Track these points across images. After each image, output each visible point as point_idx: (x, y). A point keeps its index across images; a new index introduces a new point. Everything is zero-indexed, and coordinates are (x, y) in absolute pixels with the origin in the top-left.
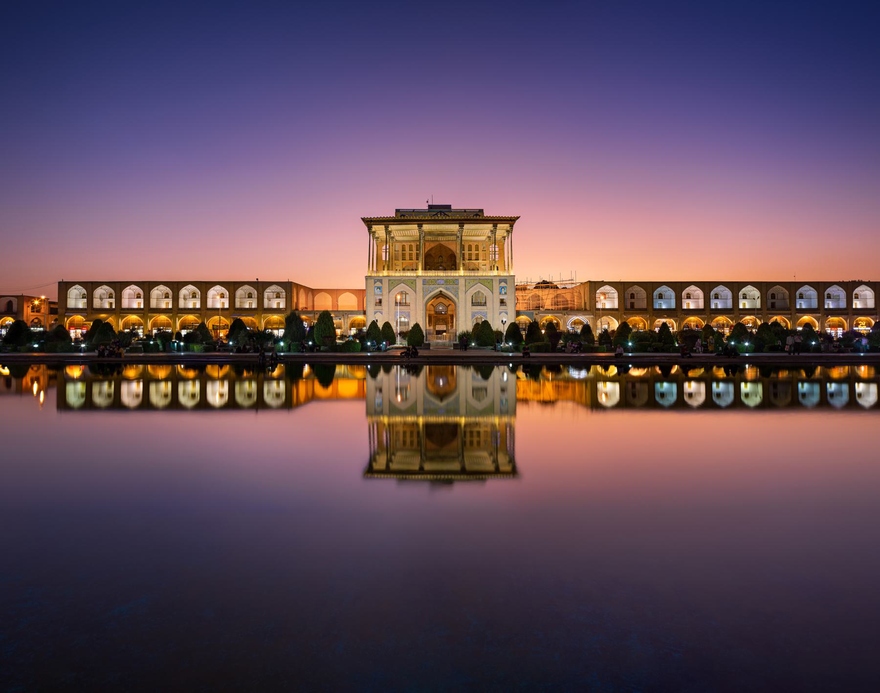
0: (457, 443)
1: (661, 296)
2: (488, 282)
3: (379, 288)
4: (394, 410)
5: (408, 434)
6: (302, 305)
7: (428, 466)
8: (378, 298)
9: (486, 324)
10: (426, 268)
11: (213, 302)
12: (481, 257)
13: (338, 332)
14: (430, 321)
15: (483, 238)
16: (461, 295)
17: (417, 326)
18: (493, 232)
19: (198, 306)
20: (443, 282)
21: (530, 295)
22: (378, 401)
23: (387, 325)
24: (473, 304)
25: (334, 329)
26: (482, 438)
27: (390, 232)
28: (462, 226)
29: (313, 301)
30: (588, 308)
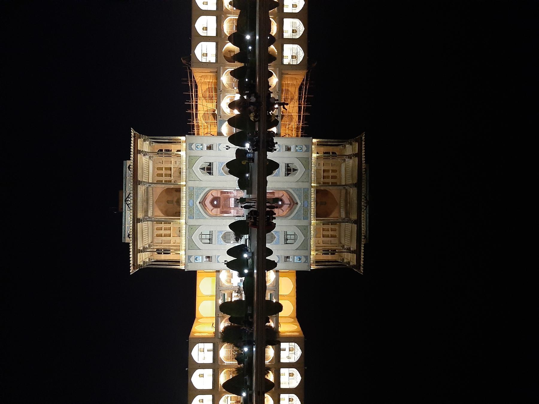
0: (333, 190)
2: (191, 161)
3: (196, 259)
4: (305, 246)
5: (326, 233)
7: (354, 217)
8: (205, 259)
9: (229, 165)
12: (168, 166)
15: (151, 163)
16: (203, 184)
17: (231, 226)
18: (145, 154)
20: (191, 201)
21: (204, 122)
22: (296, 260)
23: (230, 252)
26: (330, 168)
28: (140, 183)
29: (207, 317)
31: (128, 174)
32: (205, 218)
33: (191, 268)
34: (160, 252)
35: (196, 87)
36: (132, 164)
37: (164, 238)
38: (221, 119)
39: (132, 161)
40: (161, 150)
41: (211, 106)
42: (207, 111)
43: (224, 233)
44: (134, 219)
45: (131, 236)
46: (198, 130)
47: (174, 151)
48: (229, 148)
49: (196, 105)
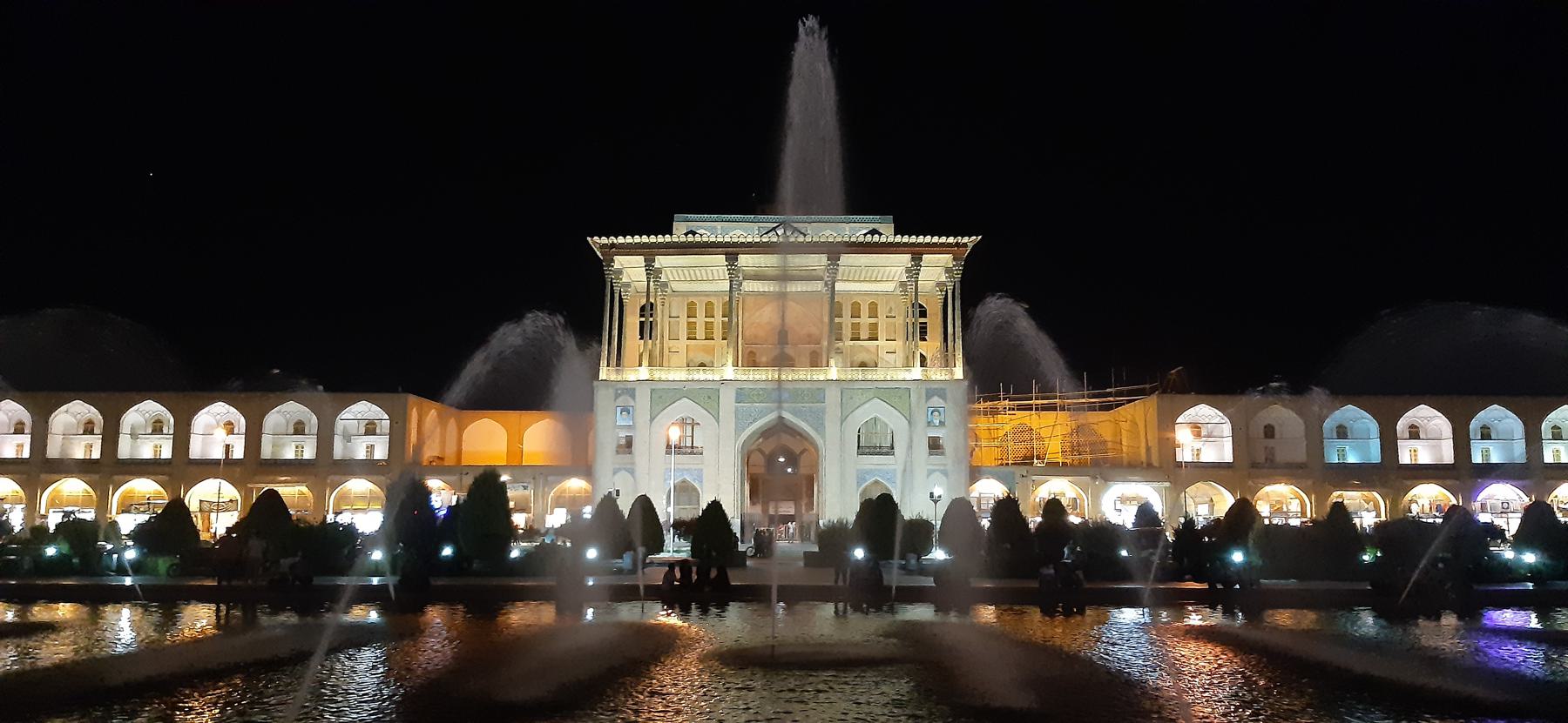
1: (1342, 433)
3: (625, 410)
6: (430, 452)
8: (623, 434)
10: (752, 361)
11: (205, 444)
12: (882, 334)
13: (519, 520)
14: (753, 493)
15: (889, 287)
16: (831, 428)
17: (715, 507)
18: (914, 272)
19: (167, 454)
21: (1007, 428)
24: (861, 450)
25: (508, 513)
27: (659, 271)
30: (1156, 464)
31: (857, 229)
32: (737, 434)
33: (603, 398)
34: (647, 313)
35: (1107, 408)
36: (883, 239)
37: (683, 320)
38: (1018, 478)
39: (891, 239)
40: (923, 314)
41: (1054, 448)
42: (1040, 438)
43: (697, 485)
44: (735, 245)
45: (690, 238)
46: (985, 414)
47: (925, 348)
48: (936, 502)
49: (1053, 408)
